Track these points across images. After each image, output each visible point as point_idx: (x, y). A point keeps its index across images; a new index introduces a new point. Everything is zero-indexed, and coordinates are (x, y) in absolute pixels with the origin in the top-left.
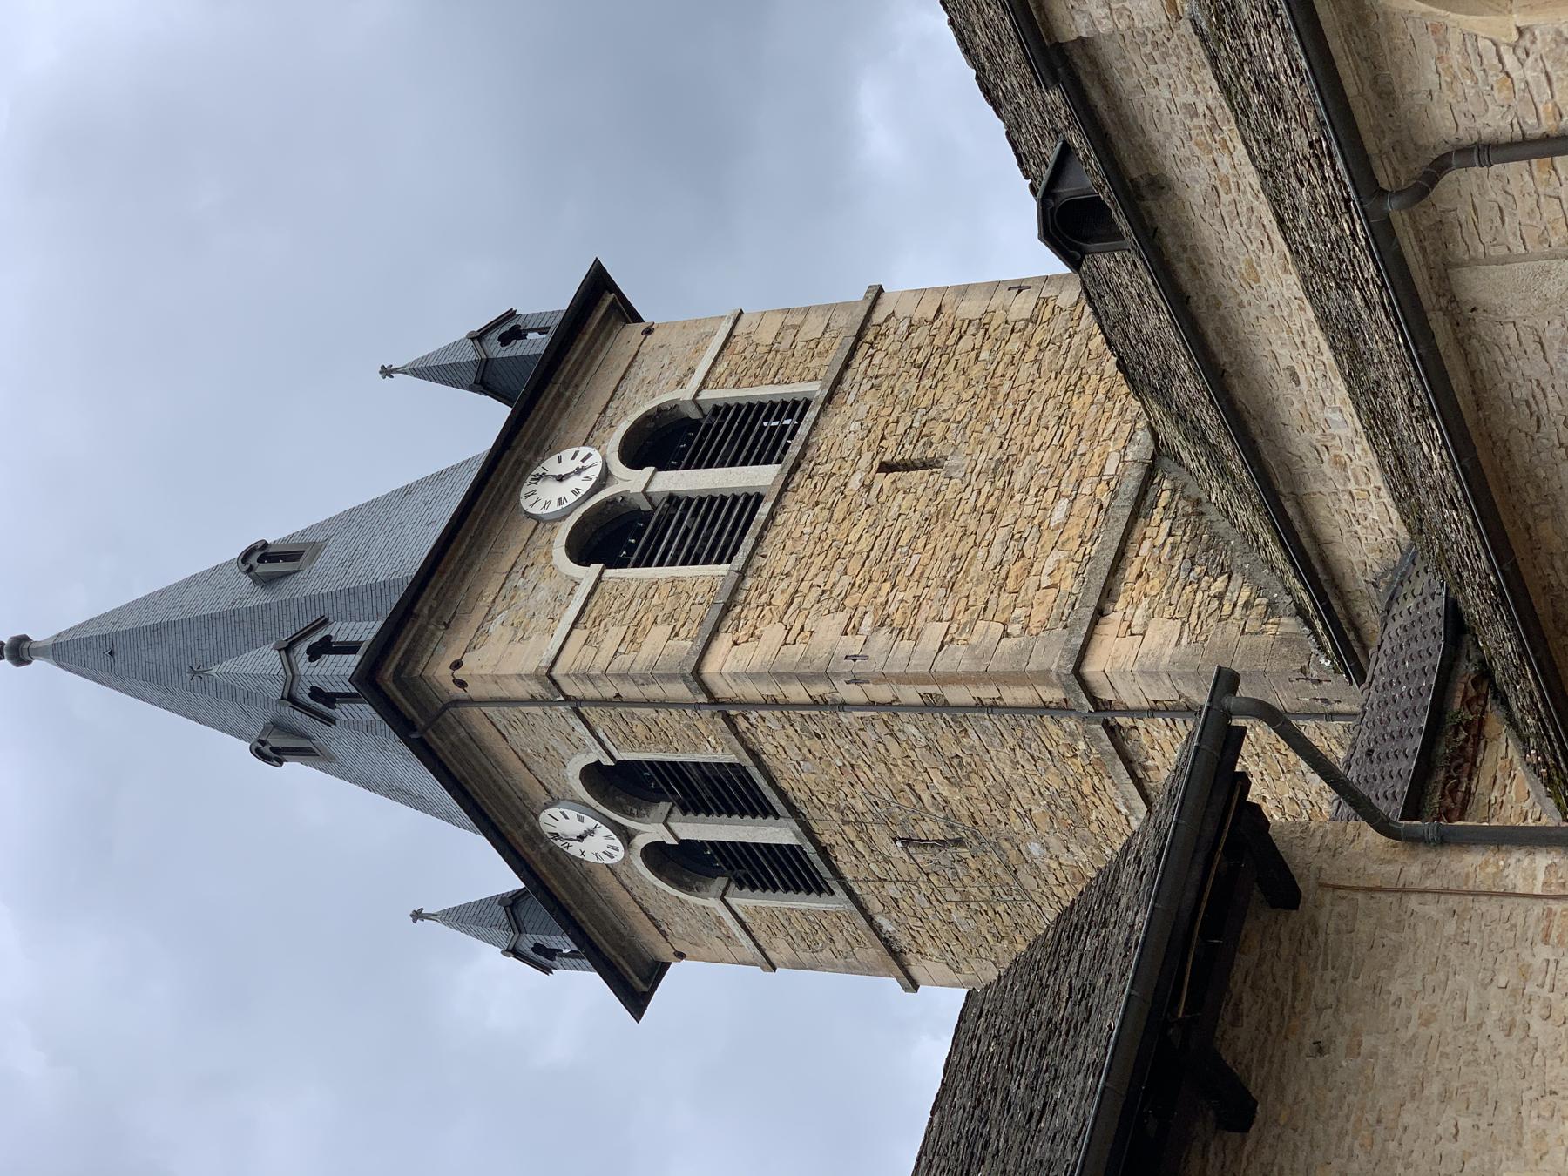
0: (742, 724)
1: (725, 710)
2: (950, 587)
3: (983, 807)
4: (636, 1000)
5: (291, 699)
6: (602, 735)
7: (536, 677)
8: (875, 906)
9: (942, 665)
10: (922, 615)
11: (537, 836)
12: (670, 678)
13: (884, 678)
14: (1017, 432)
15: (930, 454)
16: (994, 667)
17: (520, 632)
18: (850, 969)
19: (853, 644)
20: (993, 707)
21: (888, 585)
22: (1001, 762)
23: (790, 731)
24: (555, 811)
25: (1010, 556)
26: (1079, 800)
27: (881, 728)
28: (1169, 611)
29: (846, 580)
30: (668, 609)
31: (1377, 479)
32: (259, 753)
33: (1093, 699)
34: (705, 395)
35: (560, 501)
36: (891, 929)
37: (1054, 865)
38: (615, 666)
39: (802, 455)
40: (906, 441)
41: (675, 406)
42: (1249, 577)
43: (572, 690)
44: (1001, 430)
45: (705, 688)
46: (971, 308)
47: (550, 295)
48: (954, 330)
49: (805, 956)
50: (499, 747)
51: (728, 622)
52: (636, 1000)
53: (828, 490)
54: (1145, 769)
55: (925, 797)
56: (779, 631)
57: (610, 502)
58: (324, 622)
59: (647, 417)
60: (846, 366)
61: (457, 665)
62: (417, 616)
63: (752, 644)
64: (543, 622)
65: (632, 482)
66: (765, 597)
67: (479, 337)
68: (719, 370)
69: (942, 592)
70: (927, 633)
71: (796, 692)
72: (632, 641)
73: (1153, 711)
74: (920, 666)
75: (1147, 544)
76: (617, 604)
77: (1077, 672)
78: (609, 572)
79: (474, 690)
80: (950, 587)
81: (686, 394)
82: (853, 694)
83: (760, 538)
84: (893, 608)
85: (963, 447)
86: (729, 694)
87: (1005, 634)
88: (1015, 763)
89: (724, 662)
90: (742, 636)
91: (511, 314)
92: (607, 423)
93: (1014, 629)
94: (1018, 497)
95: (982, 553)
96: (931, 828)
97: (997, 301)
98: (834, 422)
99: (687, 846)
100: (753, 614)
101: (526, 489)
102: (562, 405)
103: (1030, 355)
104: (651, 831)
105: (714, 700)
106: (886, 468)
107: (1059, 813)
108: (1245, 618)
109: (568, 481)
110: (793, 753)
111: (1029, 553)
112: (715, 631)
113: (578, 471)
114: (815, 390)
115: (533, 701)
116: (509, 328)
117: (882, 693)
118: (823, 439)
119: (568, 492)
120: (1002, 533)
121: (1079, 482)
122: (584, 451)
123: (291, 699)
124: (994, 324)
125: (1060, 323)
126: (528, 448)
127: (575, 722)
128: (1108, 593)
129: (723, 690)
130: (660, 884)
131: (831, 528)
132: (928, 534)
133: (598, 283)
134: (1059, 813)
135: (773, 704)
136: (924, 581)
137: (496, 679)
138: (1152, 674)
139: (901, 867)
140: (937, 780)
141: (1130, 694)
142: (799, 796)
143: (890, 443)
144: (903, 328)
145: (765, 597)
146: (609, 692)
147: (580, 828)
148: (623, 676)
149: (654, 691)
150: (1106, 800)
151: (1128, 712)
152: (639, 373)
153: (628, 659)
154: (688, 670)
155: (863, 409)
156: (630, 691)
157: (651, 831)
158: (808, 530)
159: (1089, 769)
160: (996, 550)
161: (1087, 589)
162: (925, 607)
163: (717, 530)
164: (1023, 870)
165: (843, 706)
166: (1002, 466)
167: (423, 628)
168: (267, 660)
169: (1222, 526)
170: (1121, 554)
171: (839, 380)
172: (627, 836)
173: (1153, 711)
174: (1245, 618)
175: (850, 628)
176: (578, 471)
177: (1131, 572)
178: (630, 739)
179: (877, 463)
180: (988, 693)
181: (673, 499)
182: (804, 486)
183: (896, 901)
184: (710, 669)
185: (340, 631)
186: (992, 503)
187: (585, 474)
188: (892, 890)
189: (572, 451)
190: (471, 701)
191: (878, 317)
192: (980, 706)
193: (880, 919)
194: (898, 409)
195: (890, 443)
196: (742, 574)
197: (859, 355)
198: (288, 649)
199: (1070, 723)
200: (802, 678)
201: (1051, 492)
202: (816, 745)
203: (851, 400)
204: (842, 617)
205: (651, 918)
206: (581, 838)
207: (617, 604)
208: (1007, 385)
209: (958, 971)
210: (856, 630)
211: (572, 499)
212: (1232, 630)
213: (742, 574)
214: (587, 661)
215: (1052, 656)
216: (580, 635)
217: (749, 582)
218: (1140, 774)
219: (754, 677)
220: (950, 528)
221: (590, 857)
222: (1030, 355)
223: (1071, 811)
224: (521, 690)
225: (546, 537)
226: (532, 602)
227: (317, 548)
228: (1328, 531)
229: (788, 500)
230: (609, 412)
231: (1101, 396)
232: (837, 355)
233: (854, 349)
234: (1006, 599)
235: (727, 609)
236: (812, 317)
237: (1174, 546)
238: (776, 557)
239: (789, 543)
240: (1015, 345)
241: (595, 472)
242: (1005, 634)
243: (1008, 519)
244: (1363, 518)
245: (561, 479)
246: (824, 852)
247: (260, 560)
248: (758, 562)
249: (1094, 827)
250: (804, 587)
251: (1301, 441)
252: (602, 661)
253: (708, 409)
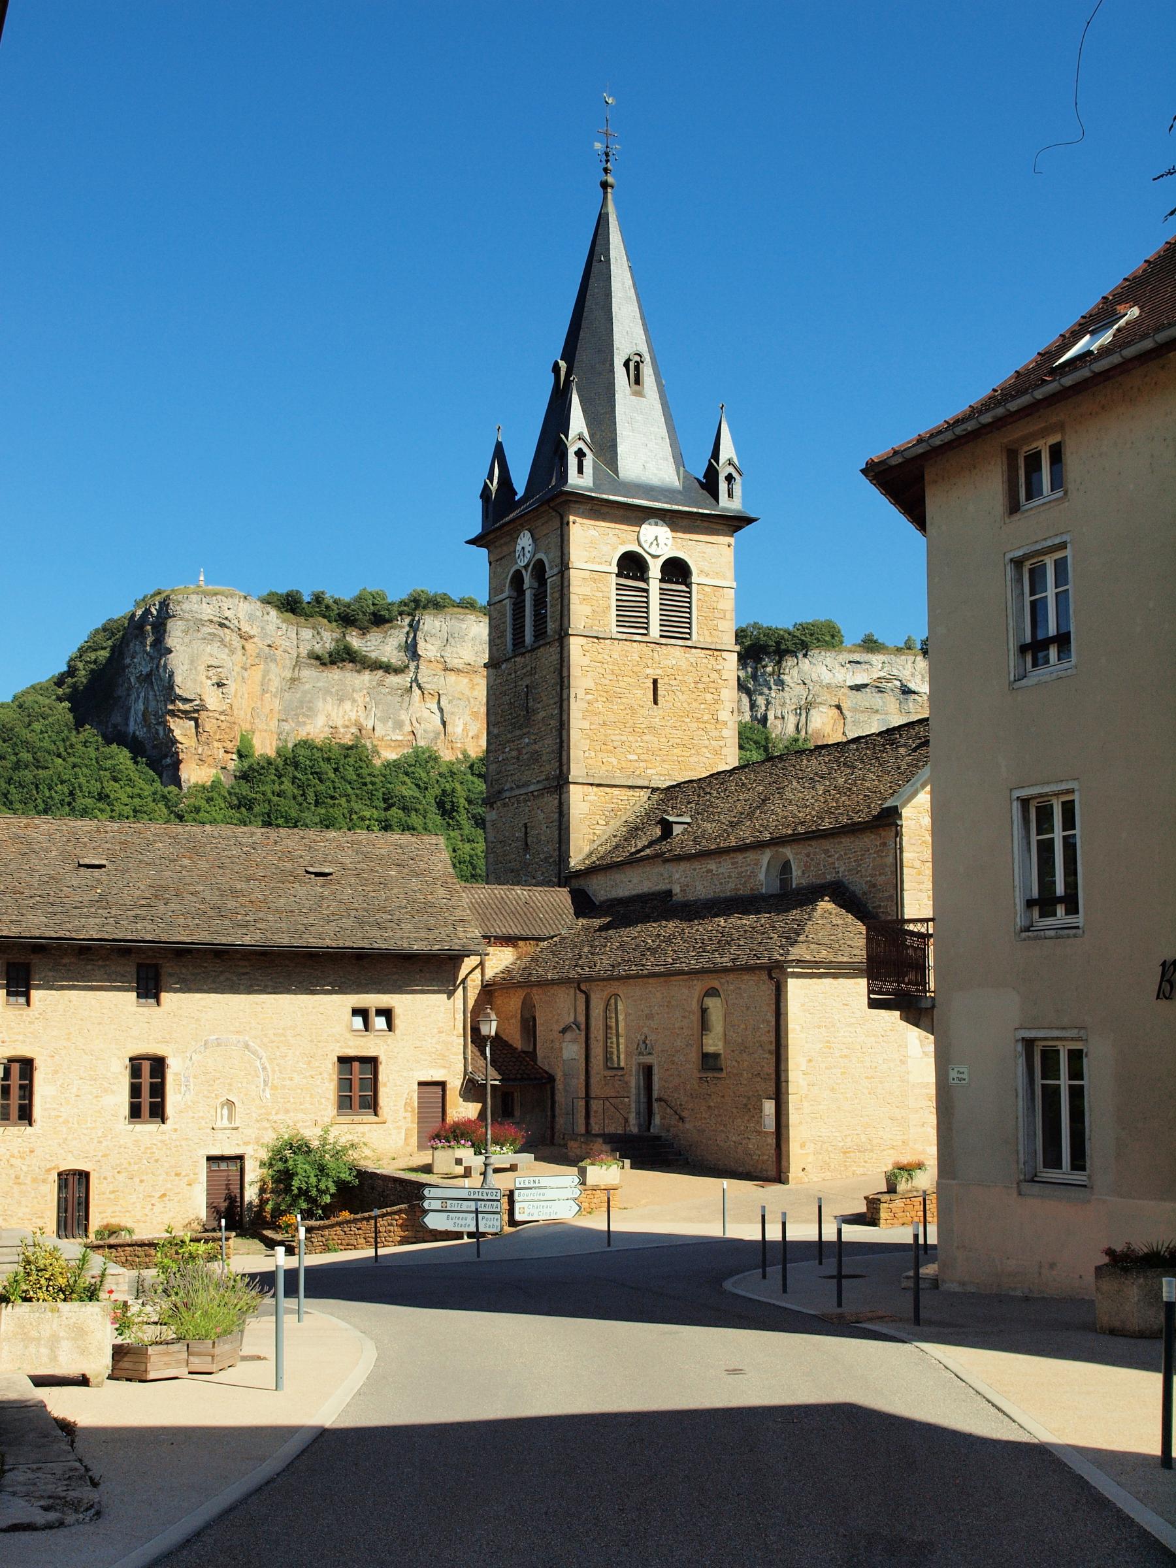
14: (668, 730)
25: (615, 744)
29: (607, 682)
63: (582, 653)
106: (655, 682)
125: (714, 733)
144: (719, 667)
160: (618, 738)
166: (652, 729)
204: (591, 685)
210: (587, 693)
222: (702, 726)
243: (630, 738)
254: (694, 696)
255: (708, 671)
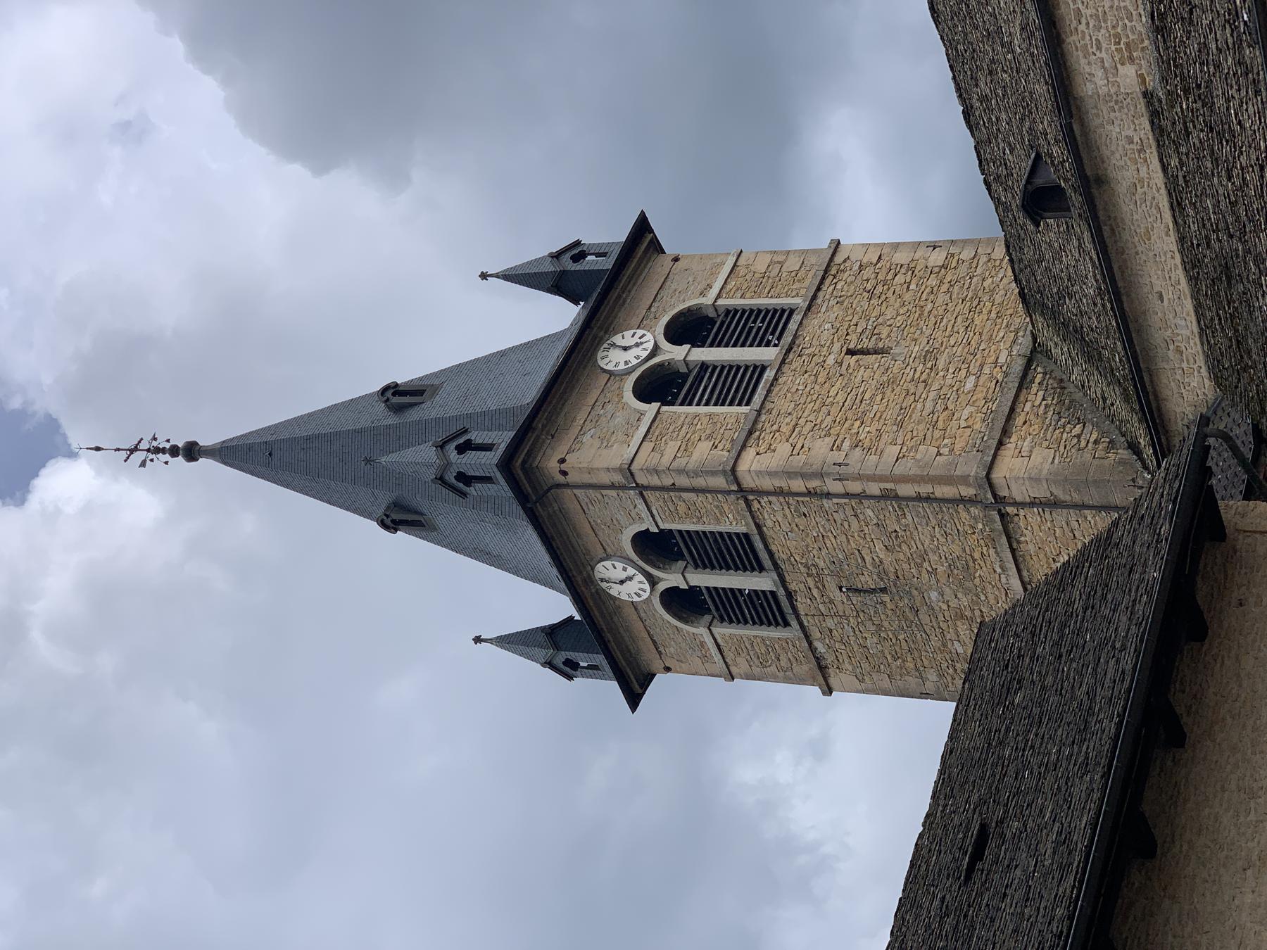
0: (756, 505)
1: (744, 493)
2: (900, 425)
3: (906, 566)
4: (634, 700)
5: (441, 479)
6: (655, 512)
7: (620, 470)
8: (815, 634)
9: (898, 470)
10: (883, 441)
11: (590, 580)
12: (714, 473)
13: (860, 477)
14: (938, 334)
15: (881, 345)
16: (932, 472)
17: (605, 442)
18: (787, 680)
19: (839, 457)
20: (928, 499)
21: (858, 423)
22: (924, 537)
23: (787, 511)
24: (608, 563)
26: (971, 564)
27: (849, 512)
28: (1045, 444)
29: (829, 419)
30: (708, 432)
31: (1201, 361)
32: (384, 525)
33: (994, 495)
34: (720, 302)
35: (626, 363)
36: (823, 651)
37: (945, 607)
38: (675, 465)
39: (793, 342)
40: (864, 337)
41: (699, 308)
42: (1096, 425)
43: (642, 479)
44: (928, 333)
45: (737, 481)
46: (902, 257)
47: (612, 232)
48: (887, 270)
49: (757, 670)
50: (579, 518)
51: (751, 441)
52: (634, 700)
53: (813, 364)
54: (1019, 542)
55: (868, 559)
56: (787, 447)
57: (661, 365)
58: (465, 431)
59: (681, 314)
60: (819, 289)
61: (562, 461)
62: (534, 429)
63: (769, 454)
64: (621, 437)
65: (676, 353)
66: (775, 427)
67: (557, 256)
68: (729, 287)
69: (895, 428)
70: (887, 451)
71: (798, 485)
72: (686, 448)
73: (1032, 504)
74: (883, 469)
75: (1029, 405)
76: (672, 428)
77: (989, 473)
78: (665, 408)
79: (573, 478)
80: (900, 425)
81: (708, 300)
82: (836, 487)
83: (769, 391)
84: (862, 437)
85: (902, 342)
86: (752, 485)
87: (939, 454)
88: (933, 537)
89: (750, 463)
90: (762, 449)
91: (577, 243)
92: (652, 316)
93: (945, 451)
94: (941, 374)
95: (919, 406)
96: (868, 581)
97: (919, 254)
98: (813, 323)
99: (694, 591)
100: (768, 437)
101: (600, 354)
102: (620, 302)
103: (944, 288)
104: (672, 579)
105: (741, 490)
106: (851, 352)
107: (956, 572)
108: (1095, 449)
109: (632, 348)
110: (785, 527)
111: (951, 407)
112: (744, 446)
113: (637, 345)
114: (799, 302)
115: (612, 486)
116: (577, 251)
117: (855, 487)
118: (806, 336)
119: (633, 357)
120: (932, 395)
121: (982, 366)
122: (640, 332)
123: (441, 479)
124: (918, 268)
125: (963, 269)
126: (601, 328)
127: (639, 502)
128: (1006, 432)
129: (748, 482)
130: (668, 617)
131: (817, 387)
132: (883, 393)
133: (642, 226)
134: (956, 572)
135: (779, 492)
136: (882, 421)
137: (590, 471)
138: (1035, 480)
139: (840, 608)
140: (879, 547)
141: (1019, 492)
142: (781, 556)
143: (853, 337)
144: (856, 267)
145: (775, 427)
146: (668, 481)
147: (623, 575)
148: (680, 471)
149: (700, 482)
150: (988, 563)
151: (1015, 504)
152: (672, 285)
153: (684, 461)
154: (728, 468)
155: (833, 316)
156: (683, 481)
157: (672, 579)
158: (801, 388)
159: (982, 542)
160: (929, 405)
161: (992, 428)
162: (885, 436)
163: (737, 385)
164: (923, 610)
165: (828, 495)
166: (929, 355)
167: (538, 437)
168: (425, 454)
169: (1078, 395)
170: (1012, 410)
171: (814, 297)
172: (653, 582)
173: (1032, 504)
174: (1095, 449)
175: (836, 447)
176: (637, 345)
177: (1019, 420)
178: (674, 515)
179: (844, 350)
180: (925, 489)
181: (704, 366)
182: (796, 363)
183: (831, 631)
184: (743, 467)
185: (477, 437)
186: (924, 376)
187: (644, 346)
188: (830, 623)
189: (632, 332)
190: (567, 486)
191: (839, 259)
192: (919, 498)
193: (817, 644)
194: (856, 317)
195: (853, 337)
196: (759, 412)
197: (827, 282)
198: (442, 446)
199: (975, 511)
200: (804, 476)
201: (964, 372)
202: (802, 522)
203: (823, 310)
204: (829, 440)
205: (654, 642)
206: (622, 582)
207: (672, 428)
208: (930, 306)
209: (862, 681)
210: (839, 449)
211: (635, 362)
212: (1087, 456)
213: (759, 412)
214: (655, 461)
215: (972, 467)
216: (648, 446)
217: (763, 418)
218: (1015, 546)
219: (772, 474)
220: (897, 390)
221: (624, 597)
222: (944, 288)
223: (962, 571)
224: (605, 479)
225: (617, 385)
226: (611, 424)
227: (435, 389)
228: (1165, 393)
229: (785, 368)
230: (653, 309)
231: (993, 315)
232: (811, 282)
233: (823, 278)
234: (937, 434)
235: (750, 433)
236: (791, 256)
237: (1046, 406)
238: (781, 403)
239: (789, 395)
240: (933, 281)
241: (650, 345)
242: (939, 454)
243: (936, 386)
244: (1188, 385)
245: (625, 349)
246: (790, 595)
247: (394, 394)
248: (768, 405)
249: (977, 581)
250: (802, 422)
251: (1158, 336)
252: (666, 461)
253: (721, 311)
254: (892, 299)
255: (858, 282)
